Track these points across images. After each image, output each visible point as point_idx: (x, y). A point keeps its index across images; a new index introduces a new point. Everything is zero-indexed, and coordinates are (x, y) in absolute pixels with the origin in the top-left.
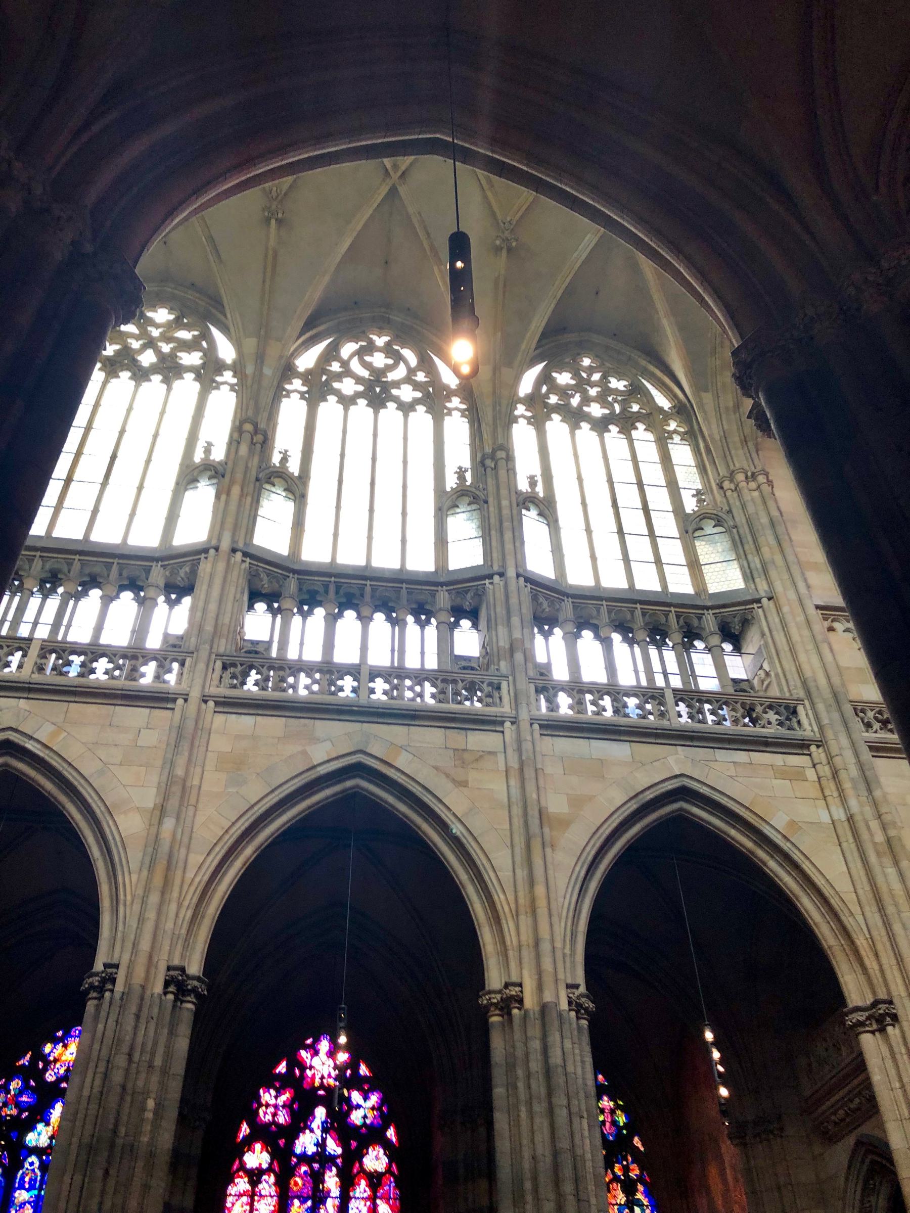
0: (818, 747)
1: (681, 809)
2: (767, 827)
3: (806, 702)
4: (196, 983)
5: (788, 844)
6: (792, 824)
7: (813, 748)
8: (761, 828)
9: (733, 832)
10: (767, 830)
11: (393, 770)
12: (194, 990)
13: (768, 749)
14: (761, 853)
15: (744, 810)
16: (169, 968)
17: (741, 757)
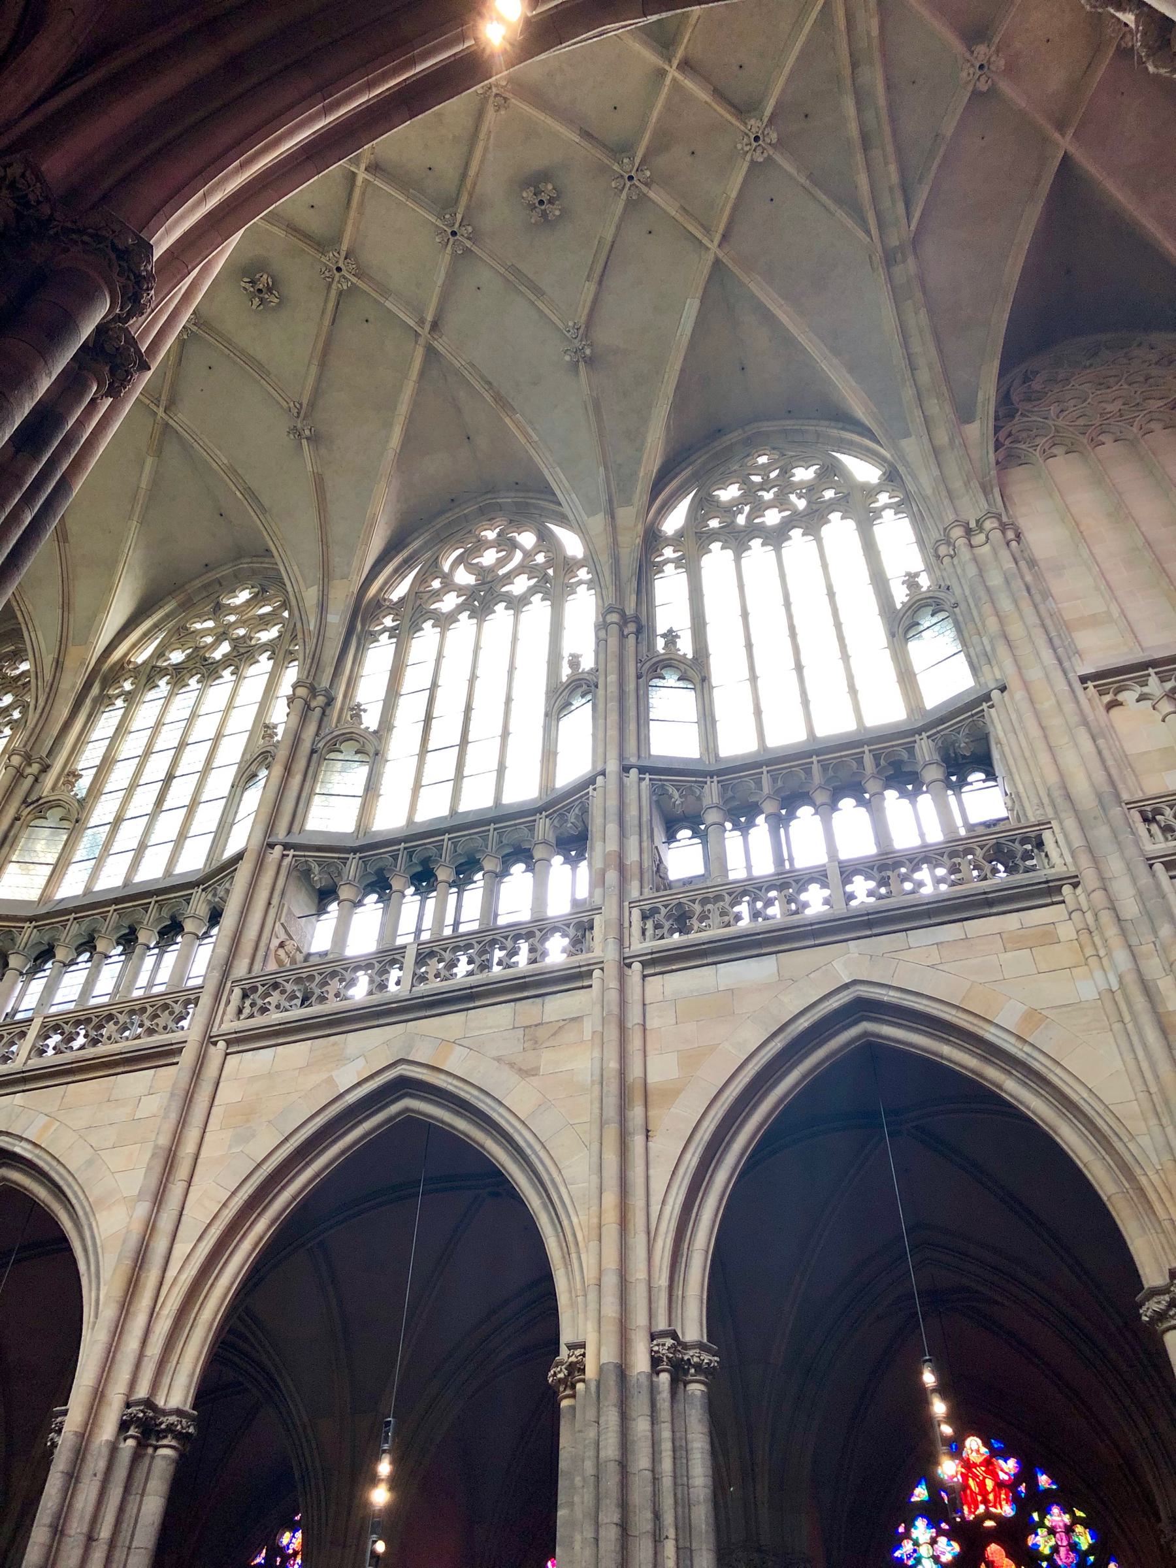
0: (1075, 886)
1: (866, 1034)
2: (993, 1030)
3: (1054, 824)
4: (173, 1419)
5: (1027, 1048)
6: (1033, 1016)
7: (1067, 890)
8: (981, 1032)
9: (946, 1050)
10: (990, 1034)
11: (443, 1076)
12: (170, 1429)
13: (994, 910)
14: (992, 1073)
15: (954, 1012)
16: (128, 1405)
17: (952, 932)
